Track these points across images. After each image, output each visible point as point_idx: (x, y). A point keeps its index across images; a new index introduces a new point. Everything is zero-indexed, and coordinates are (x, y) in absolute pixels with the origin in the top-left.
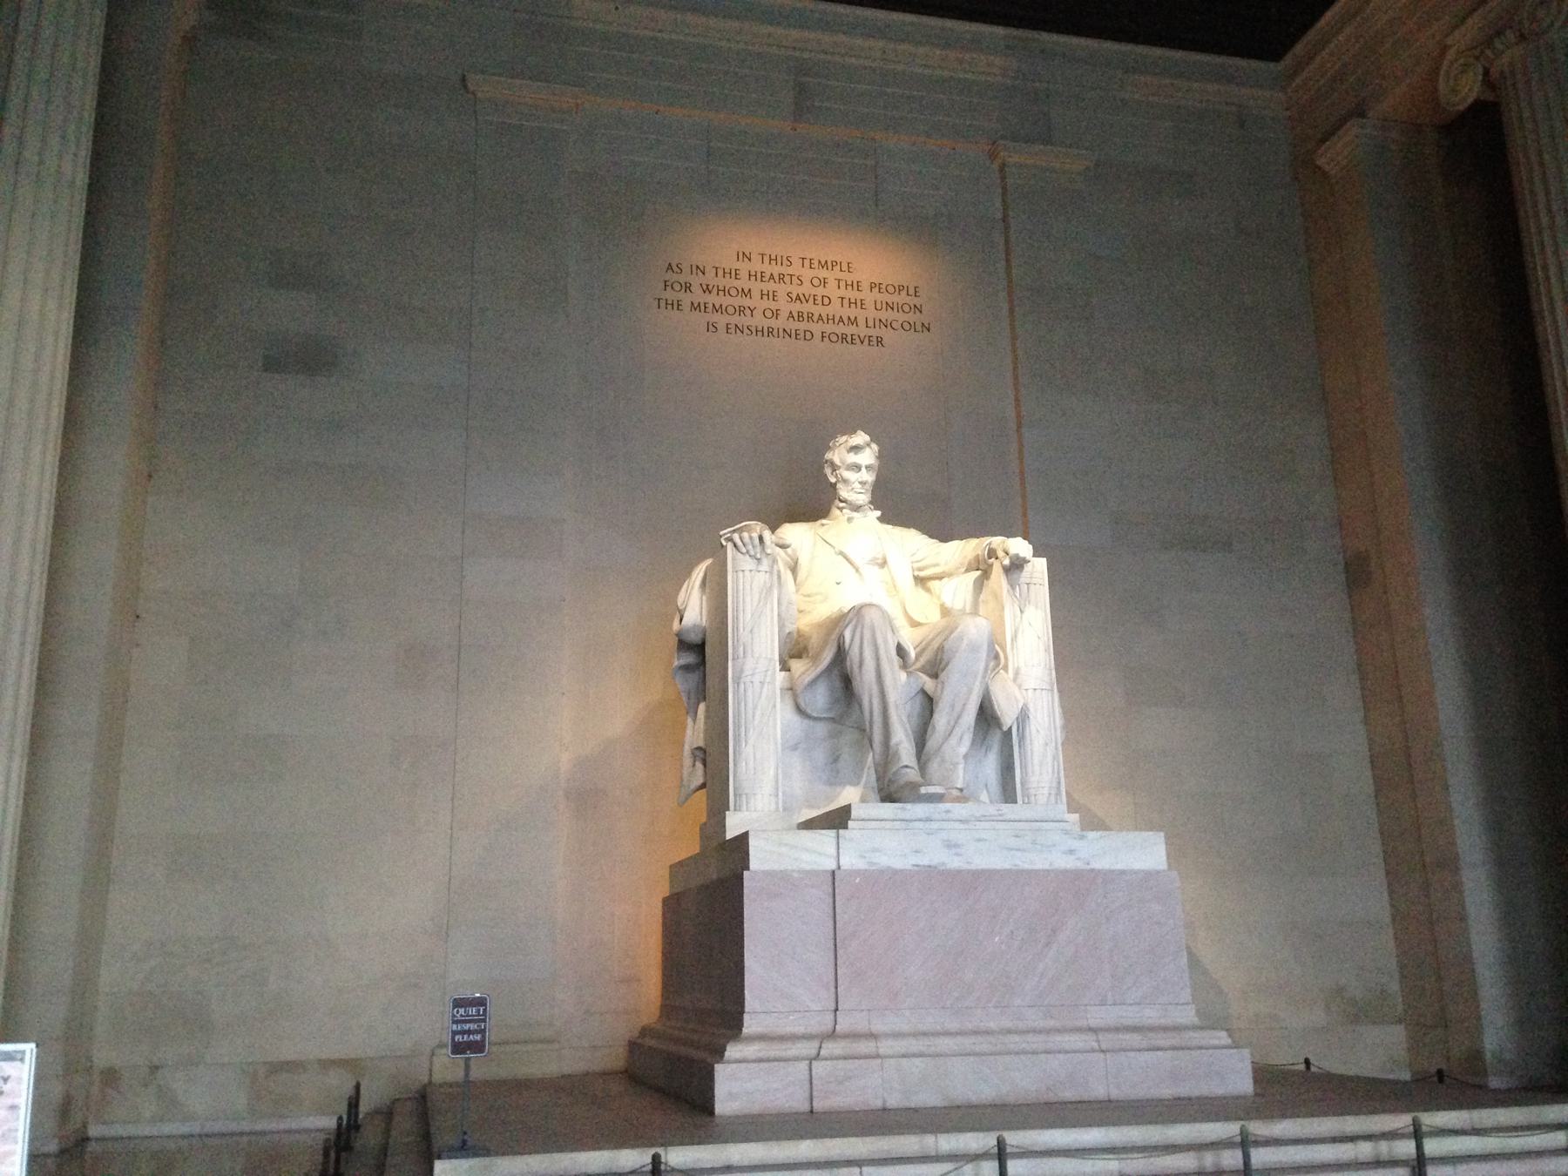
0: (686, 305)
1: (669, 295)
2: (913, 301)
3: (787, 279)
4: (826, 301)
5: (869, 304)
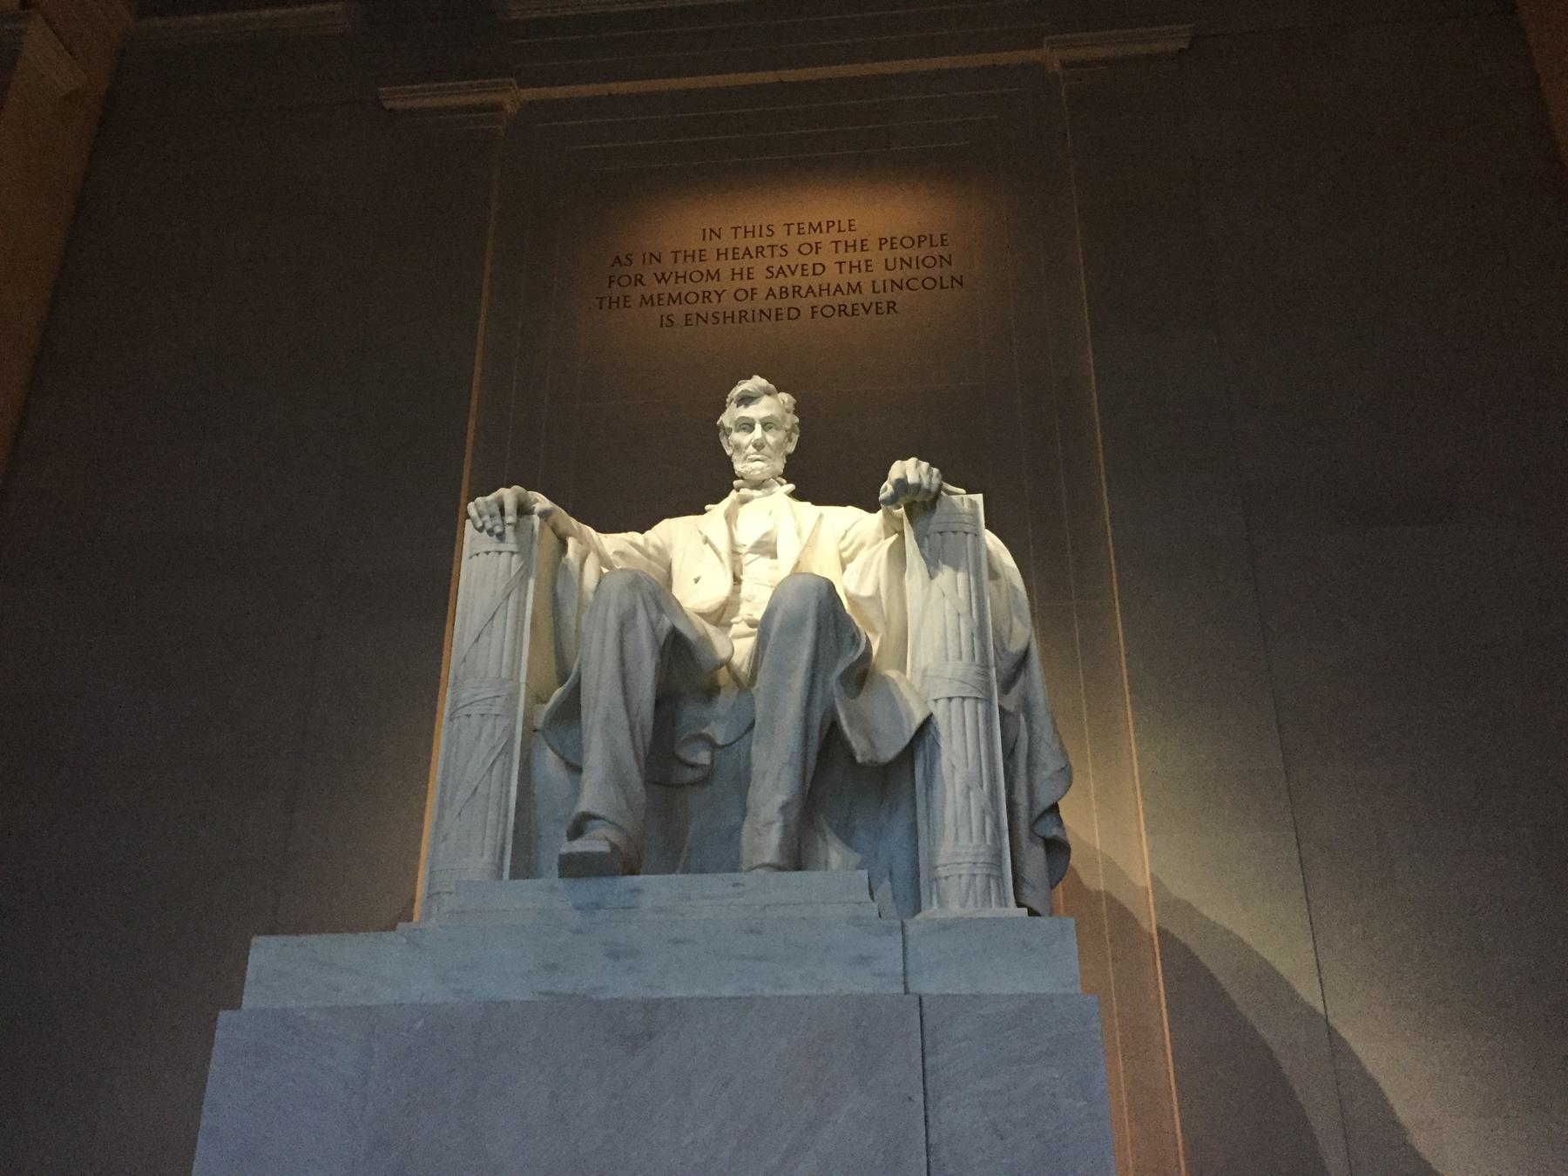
1: (616, 291)
3: (767, 252)
4: (819, 269)
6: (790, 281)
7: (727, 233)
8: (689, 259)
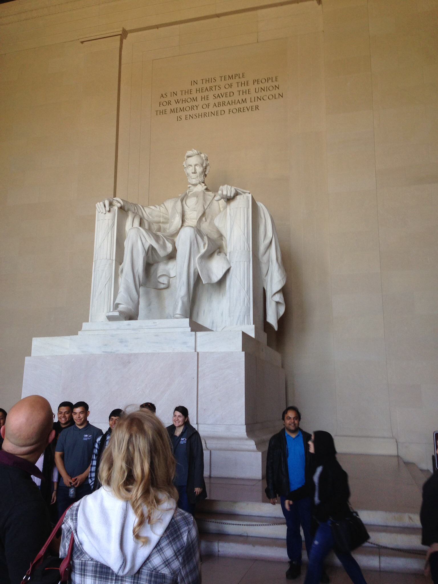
0: (168, 111)
1: (162, 108)
2: (274, 84)
3: (214, 88)
4: (232, 94)
5: (252, 91)
6: (221, 100)
7: (199, 82)
8: (186, 93)
